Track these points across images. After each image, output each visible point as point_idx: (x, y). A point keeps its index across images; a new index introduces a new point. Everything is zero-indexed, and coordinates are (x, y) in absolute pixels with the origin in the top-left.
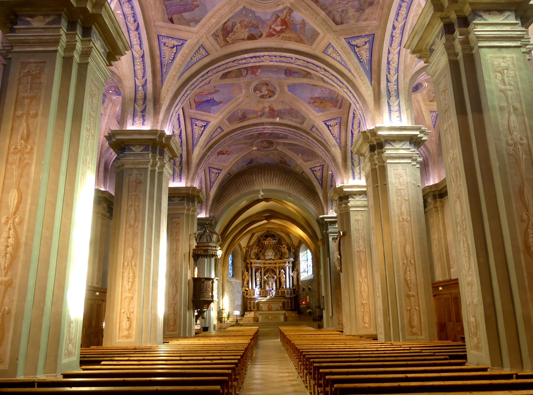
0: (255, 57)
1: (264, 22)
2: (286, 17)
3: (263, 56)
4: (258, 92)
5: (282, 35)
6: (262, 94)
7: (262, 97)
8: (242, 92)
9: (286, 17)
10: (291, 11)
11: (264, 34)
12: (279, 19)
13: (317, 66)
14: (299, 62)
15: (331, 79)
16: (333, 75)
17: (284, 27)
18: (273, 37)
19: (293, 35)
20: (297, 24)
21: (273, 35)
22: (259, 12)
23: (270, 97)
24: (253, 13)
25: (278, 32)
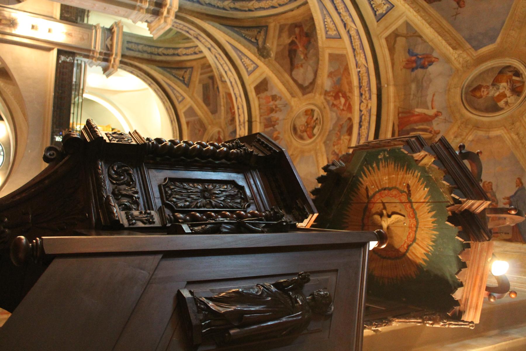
0: (361, 121)
1: (339, 119)
2: (332, 96)
3: (361, 111)
4: (501, 104)
5: (348, 94)
6: (508, 93)
7: (517, 91)
8: (497, 137)
9: (332, 96)
10: (326, 93)
11: (349, 115)
12: (335, 102)
13: (350, 37)
14: (361, 60)
15: (347, 10)
16: (339, 14)
17: (341, 95)
18: (351, 103)
19: (345, 81)
20: (334, 81)
21: (350, 104)
22: (329, 126)
23: (517, 73)
24: (330, 132)
25: (346, 100)
